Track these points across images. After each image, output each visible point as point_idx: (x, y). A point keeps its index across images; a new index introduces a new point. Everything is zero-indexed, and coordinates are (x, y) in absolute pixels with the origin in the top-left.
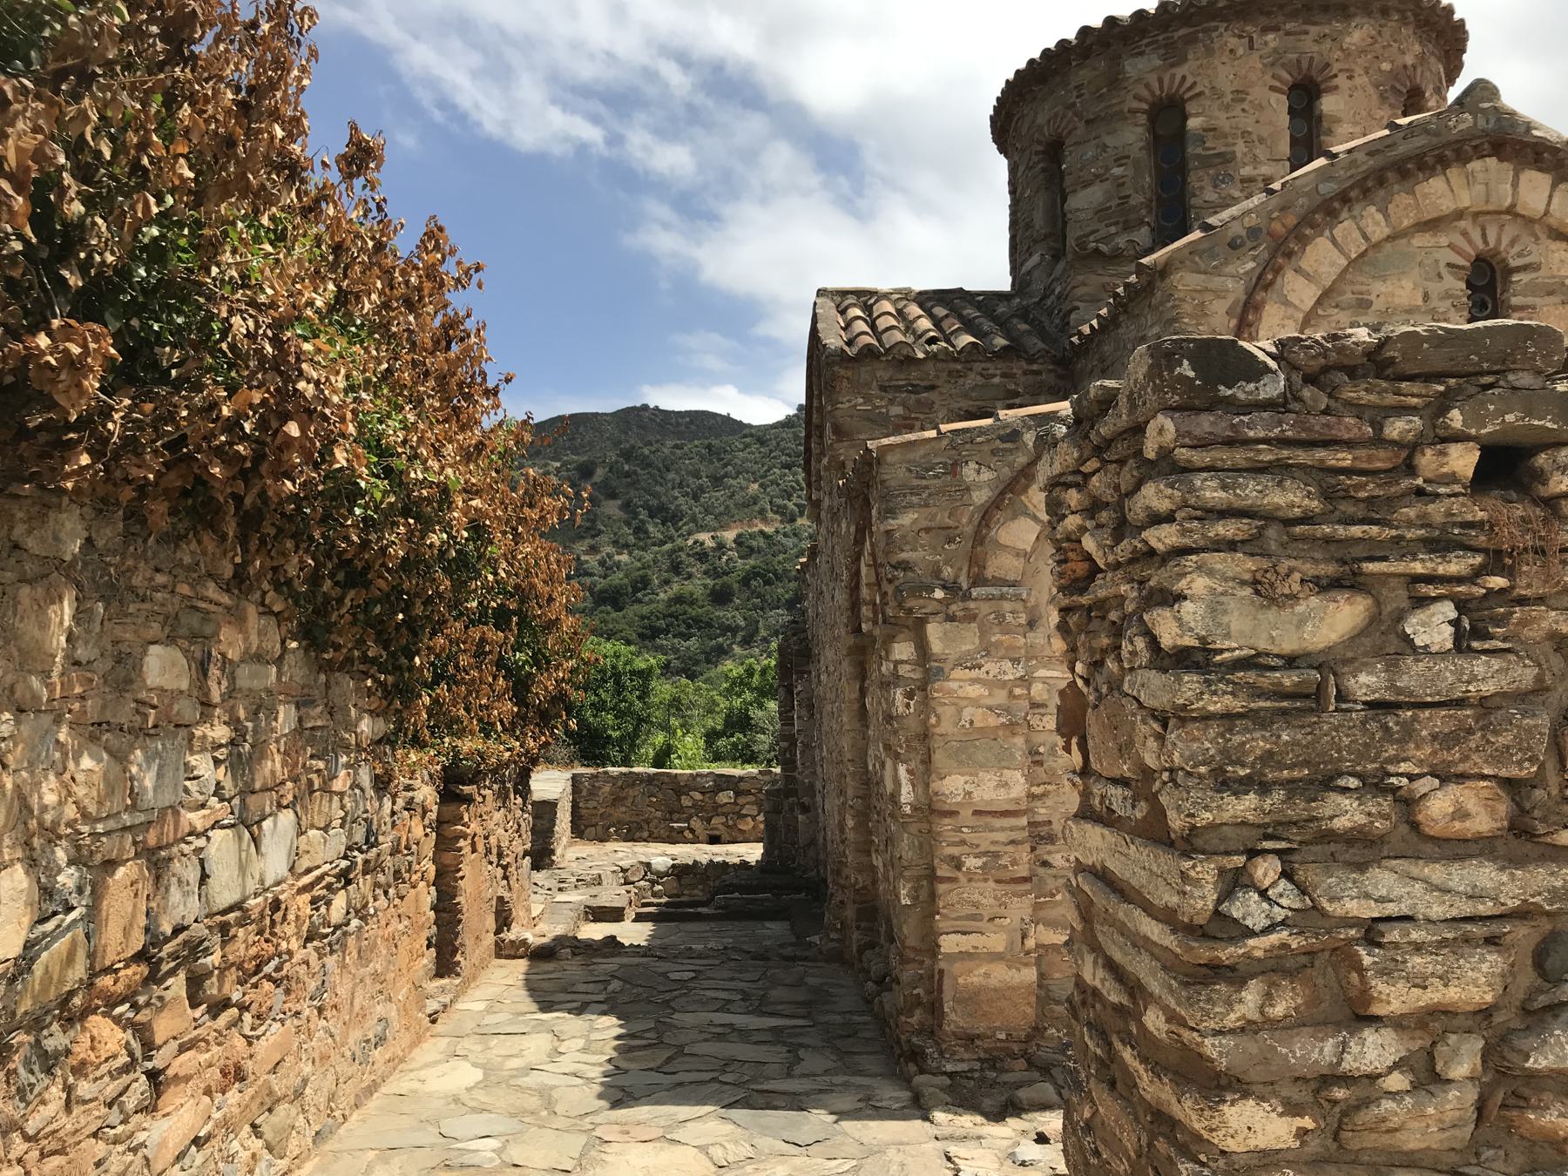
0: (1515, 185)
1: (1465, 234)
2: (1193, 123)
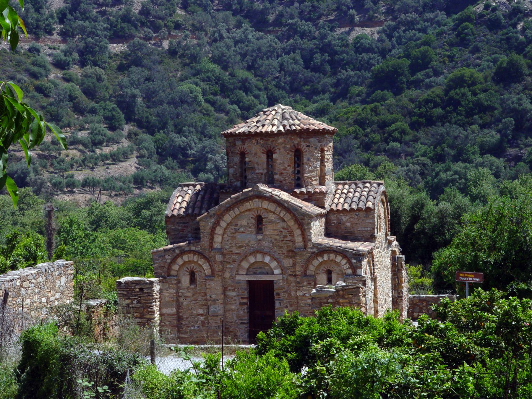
0: (262, 203)
2: (247, 159)
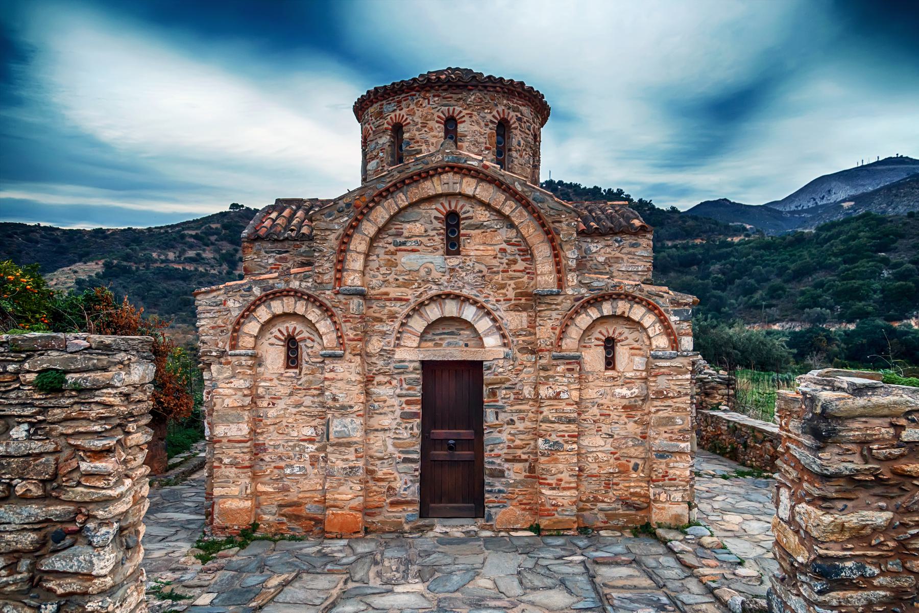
1: (442, 204)
2: (406, 136)
